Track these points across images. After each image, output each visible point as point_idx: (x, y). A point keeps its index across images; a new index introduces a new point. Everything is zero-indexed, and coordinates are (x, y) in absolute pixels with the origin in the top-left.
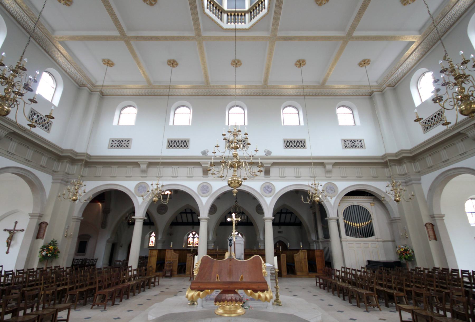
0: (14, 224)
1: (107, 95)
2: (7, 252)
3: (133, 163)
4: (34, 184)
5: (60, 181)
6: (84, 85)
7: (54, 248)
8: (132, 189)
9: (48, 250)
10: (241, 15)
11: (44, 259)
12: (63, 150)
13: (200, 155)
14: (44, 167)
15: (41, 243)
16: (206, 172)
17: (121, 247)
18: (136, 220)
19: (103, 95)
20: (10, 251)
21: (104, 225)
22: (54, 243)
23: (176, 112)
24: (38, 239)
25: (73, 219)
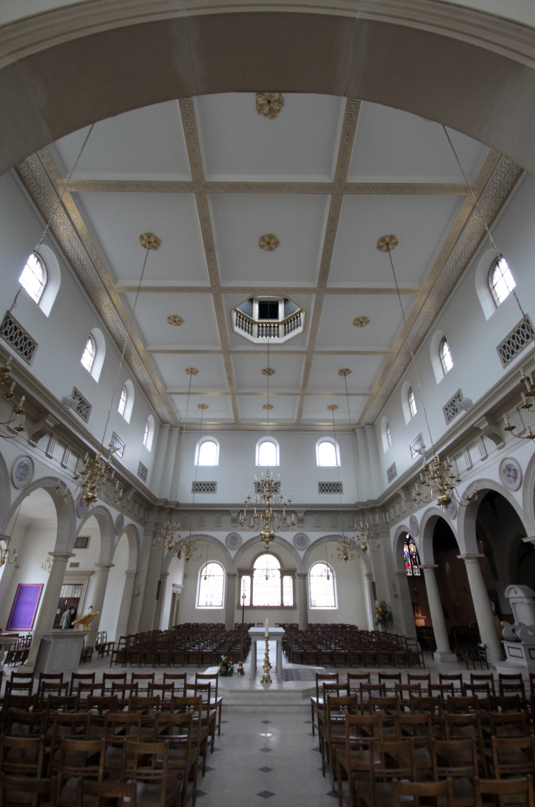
1: (374, 422)
22: (383, 606)
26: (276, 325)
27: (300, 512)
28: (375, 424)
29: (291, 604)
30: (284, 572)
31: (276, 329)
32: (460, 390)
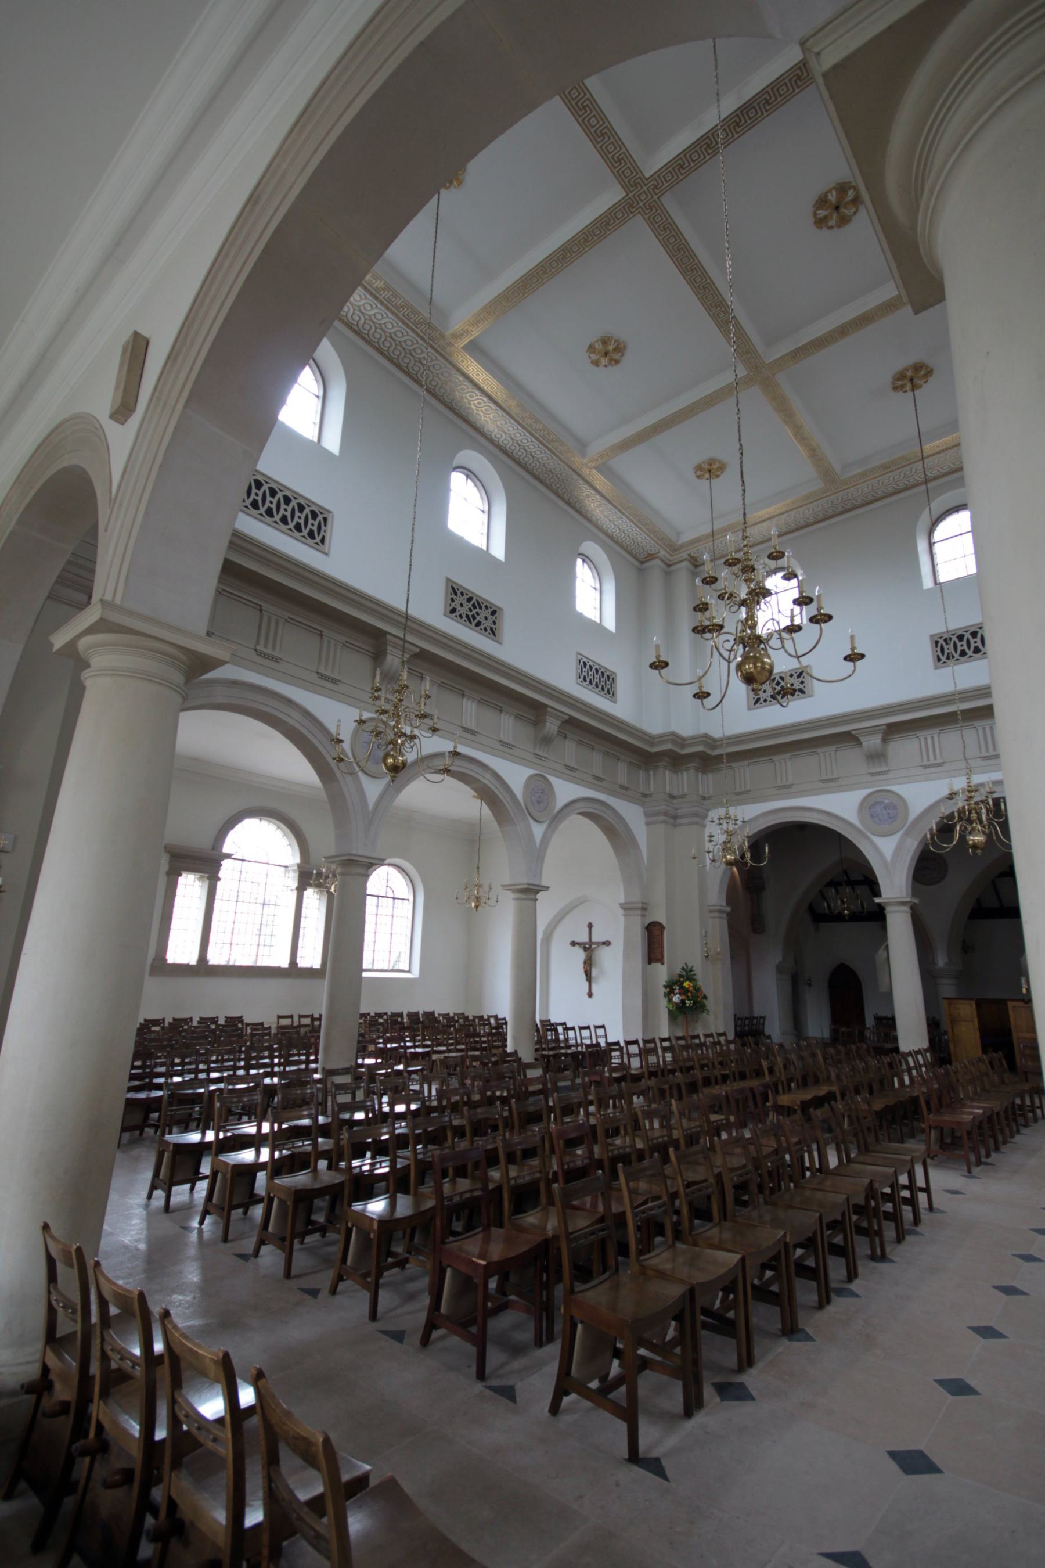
0: (587, 929)
2: (590, 995)
3: (836, 736)
4: (614, 830)
5: (662, 818)
6: (651, 557)
7: (694, 987)
8: (853, 817)
9: (684, 991)
11: (678, 1012)
12: (653, 737)
15: (662, 973)
17: (810, 985)
18: (888, 909)
20: (594, 991)
21: (757, 924)
22: (688, 974)
23: (937, 535)
24: (653, 965)
25: (710, 911)
29: (317, 964)
30: (307, 878)
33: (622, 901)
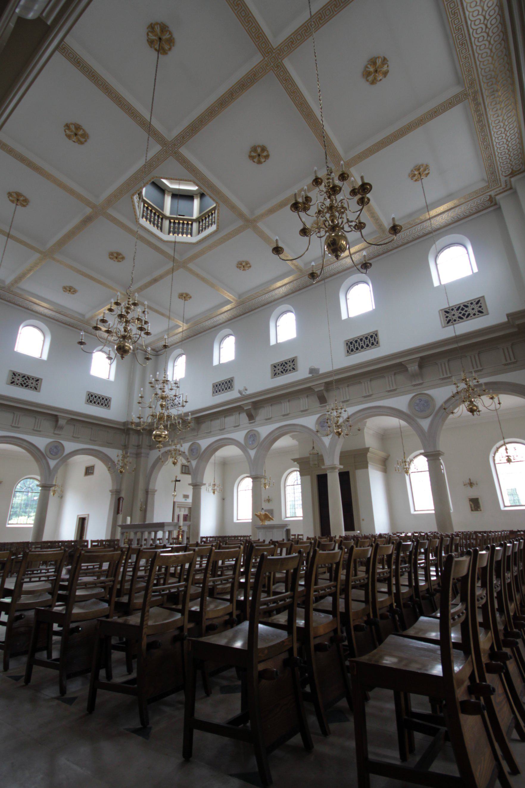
10: (188, 224)
13: (239, 395)
14: (111, 444)
16: (251, 417)
19: (157, 352)
26: (190, 223)
27: (64, 418)
28: (159, 352)
31: (190, 226)
32: (296, 357)
33: (111, 489)
